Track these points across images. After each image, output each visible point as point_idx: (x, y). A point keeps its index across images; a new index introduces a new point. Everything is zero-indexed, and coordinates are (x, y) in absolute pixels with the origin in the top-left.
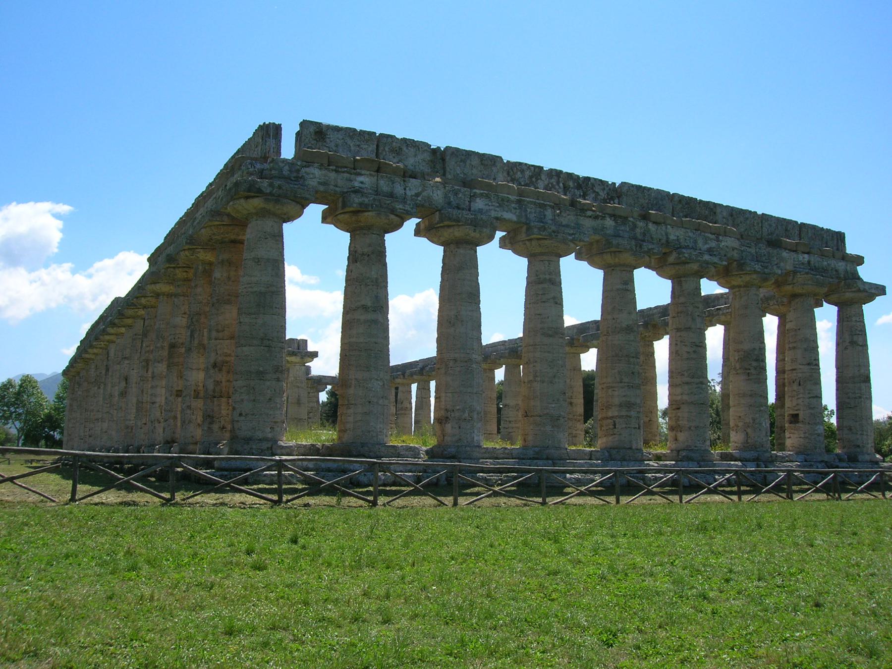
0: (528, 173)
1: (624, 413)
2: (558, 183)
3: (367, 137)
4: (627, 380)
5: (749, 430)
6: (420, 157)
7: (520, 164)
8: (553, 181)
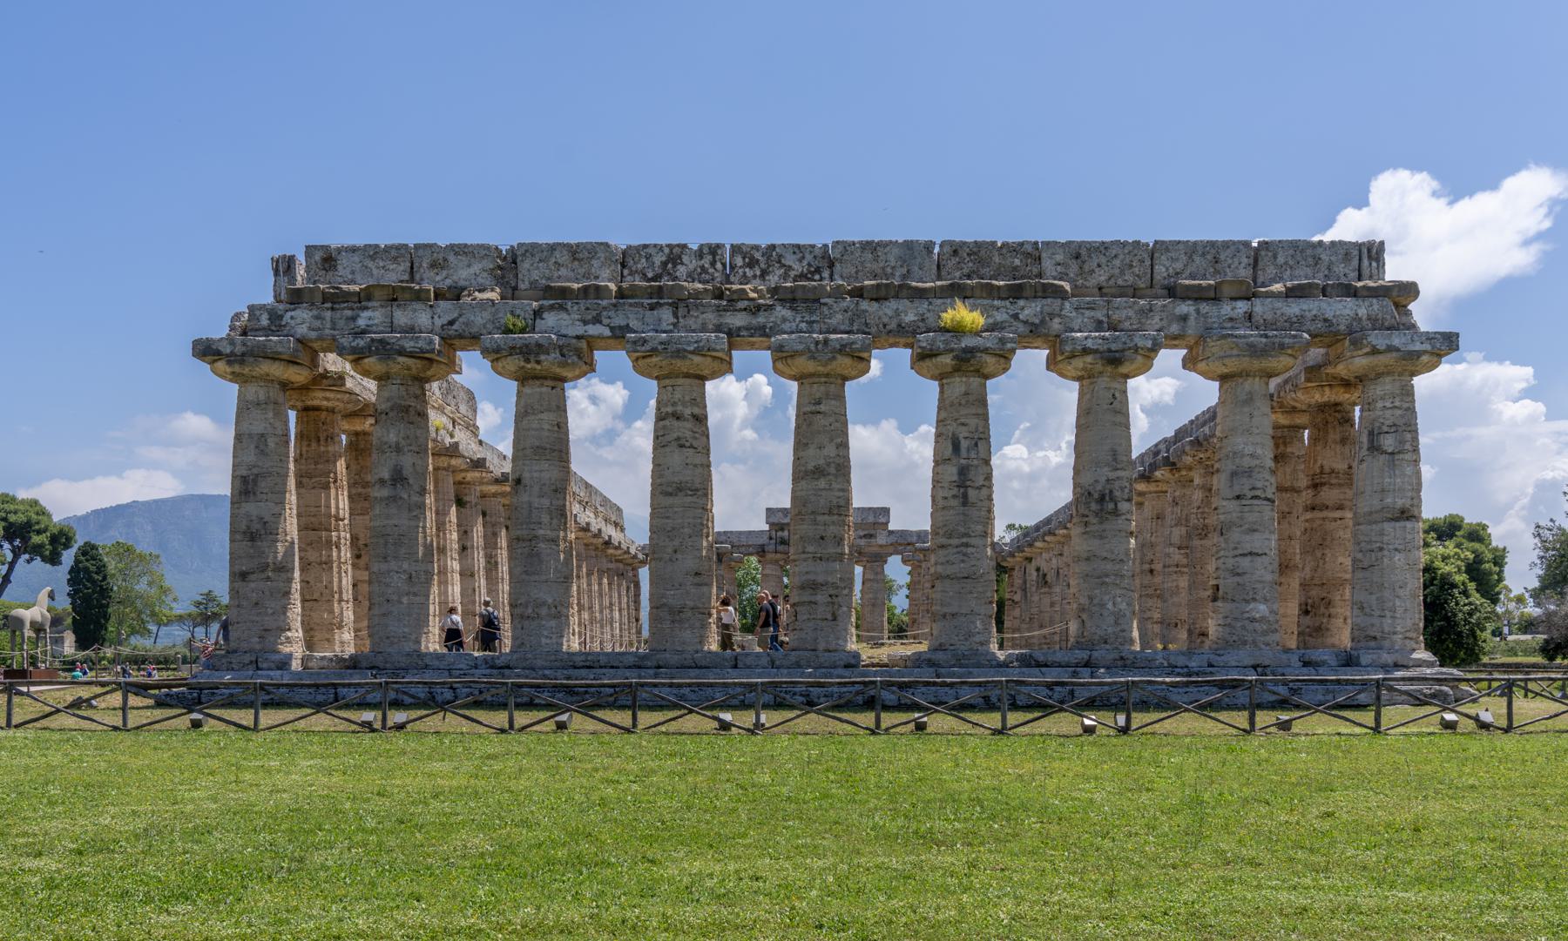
0: (658, 259)
1: (805, 599)
2: (713, 264)
3: (394, 253)
4: (810, 549)
5: (1084, 616)
6: (476, 268)
7: (645, 246)
8: (706, 262)
